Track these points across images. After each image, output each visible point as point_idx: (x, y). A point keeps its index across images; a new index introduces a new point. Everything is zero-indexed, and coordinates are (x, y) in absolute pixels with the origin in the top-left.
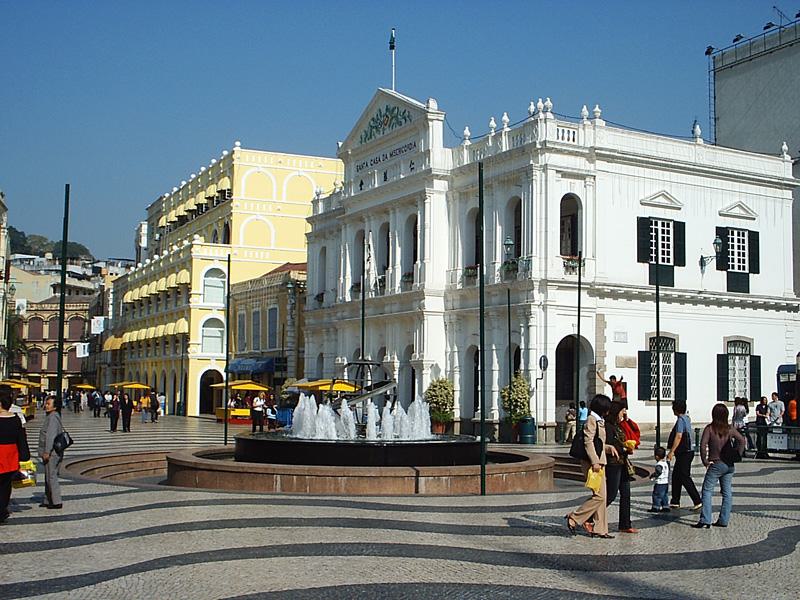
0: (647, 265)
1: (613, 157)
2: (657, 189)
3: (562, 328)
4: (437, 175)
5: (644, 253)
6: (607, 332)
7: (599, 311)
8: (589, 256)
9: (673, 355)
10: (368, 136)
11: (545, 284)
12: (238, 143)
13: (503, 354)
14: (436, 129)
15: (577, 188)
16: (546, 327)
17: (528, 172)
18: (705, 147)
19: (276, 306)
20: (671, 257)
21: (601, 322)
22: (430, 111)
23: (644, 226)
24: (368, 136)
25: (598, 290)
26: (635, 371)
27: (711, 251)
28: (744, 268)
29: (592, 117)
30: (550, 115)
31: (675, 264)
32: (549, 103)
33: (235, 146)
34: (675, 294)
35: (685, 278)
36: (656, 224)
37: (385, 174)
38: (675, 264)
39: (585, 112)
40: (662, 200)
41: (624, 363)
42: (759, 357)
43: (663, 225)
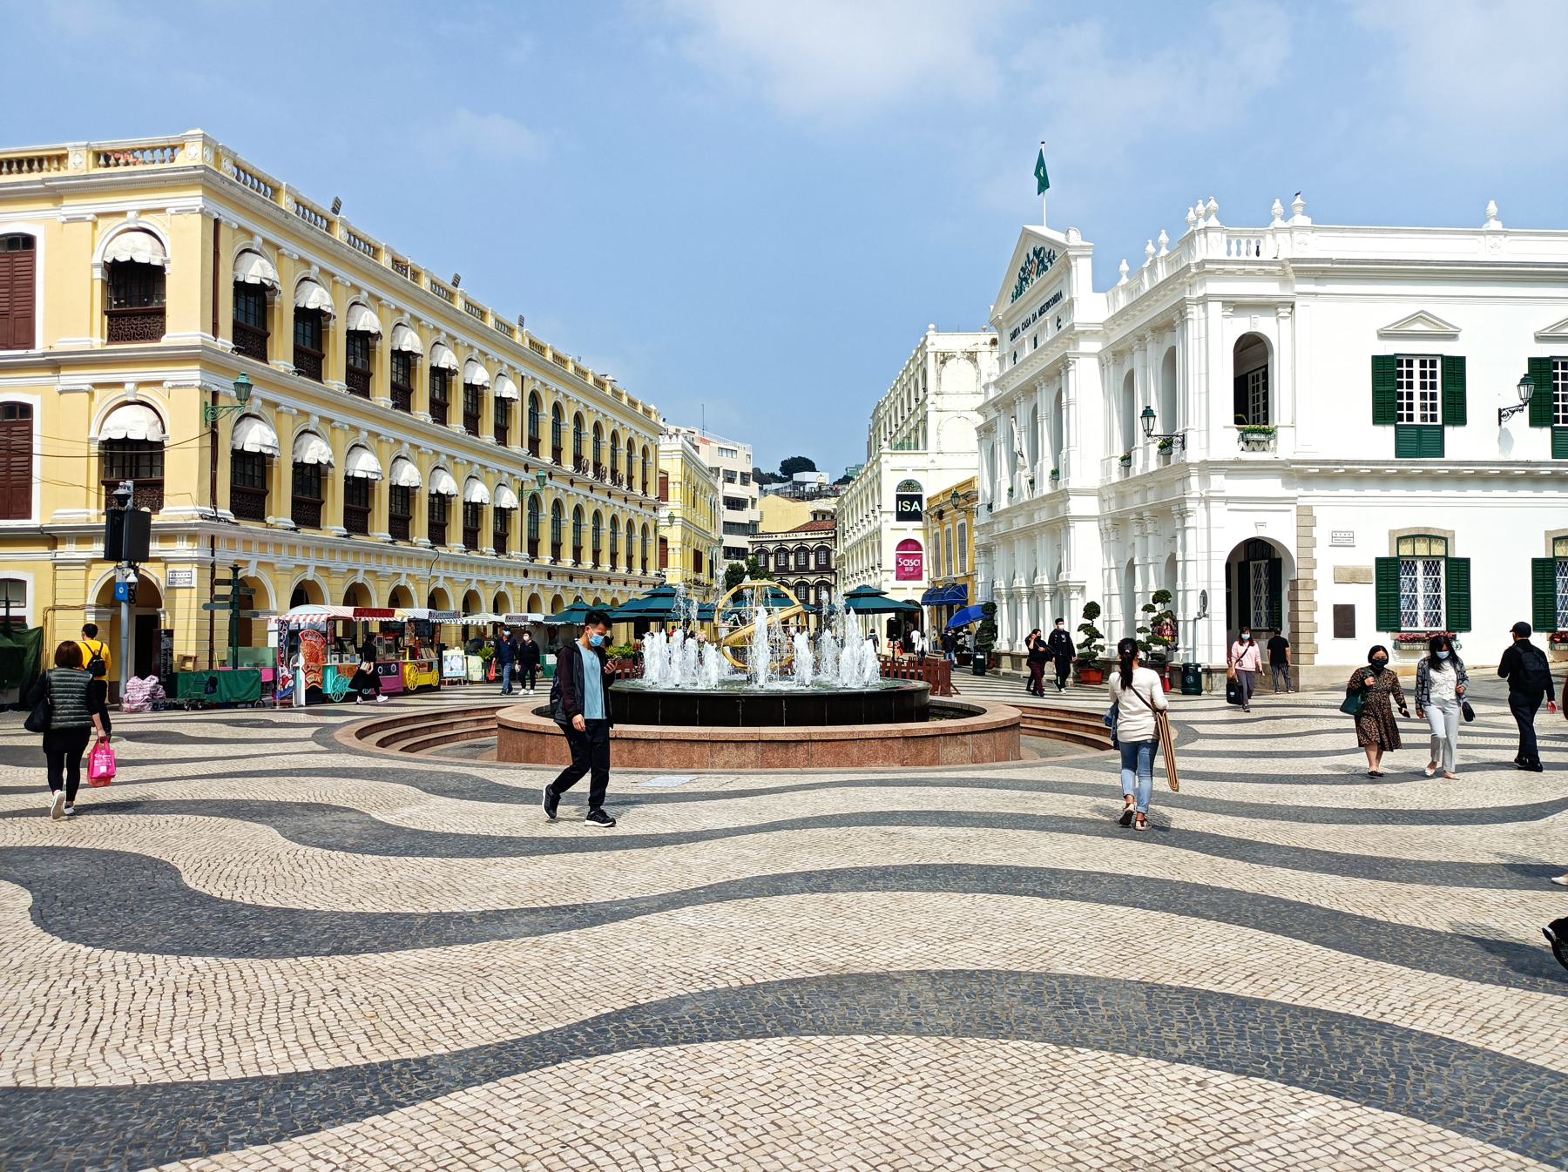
0: (1547, 432)
1: (1324, 270)
2: (1411, 308)
3: (1233, 530)
4: (1084, 332)
5: (1386, 407)
6: (1316, 532)
7: (1301, 501)
8: (1286, 420)
9: (1443, 563)
10: (1019, 291)
11: (1209, 467)
12: (932, 326)
13: (1163, 567)
14: (1082, 270)
15: (1264, 325)
16: (1209, 528)
17: (1181, 309)
18: (1505, 234)
19: (964, 521)
20: (1439, 412)
21: (1306, 520)
22: (194, 198)
23: (1387, 372)
24: (1019, 291)
25: (1297, 471)
26: (1371, 590)
27: (1513, 395)
28: (1434, 418)
29: (1287, 216)
30: (1213, 222)
31: (1446, 421)
32: (1213, 204)
33: (928, 330)
34: (1443, 469)
35: (1459, 444)
36: (1410, 364)
37: (1035, 339)
38: (1446, 421)
39: (1277, 206)
40: (1418, 327)
41: (1348, 577)
42: (1467, 561)
43: (1423, 364)
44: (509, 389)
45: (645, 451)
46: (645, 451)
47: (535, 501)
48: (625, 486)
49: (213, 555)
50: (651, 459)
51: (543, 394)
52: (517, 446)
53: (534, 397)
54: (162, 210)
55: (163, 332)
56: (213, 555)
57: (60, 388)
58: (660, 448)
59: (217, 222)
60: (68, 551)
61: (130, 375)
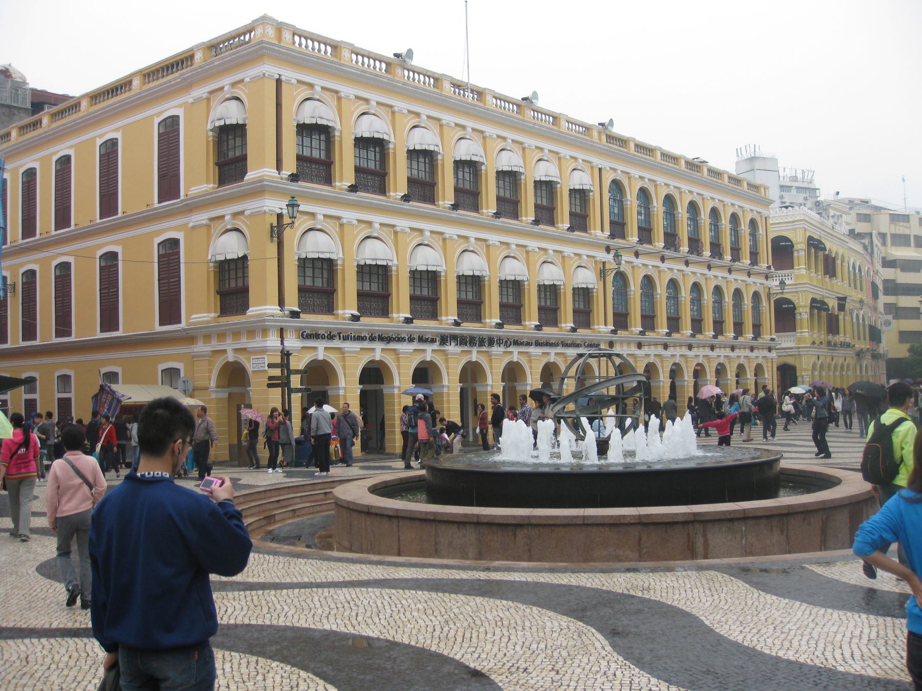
44: (581, 180)
45: (753, 223)
46: (753, 223)
47: (621, 277)
48: (728, 257)
49: (282, 343)
50: (761, 231)
51: (625, 182)
52: (599, 233)
53: (617, 185)
54: (242, 81)
55: (244, 172)
56: (282, 343)
57: (191, 225)
58: (771, 221)
59: (279, 82)
60: (201, 347)
61: (227, 210)
